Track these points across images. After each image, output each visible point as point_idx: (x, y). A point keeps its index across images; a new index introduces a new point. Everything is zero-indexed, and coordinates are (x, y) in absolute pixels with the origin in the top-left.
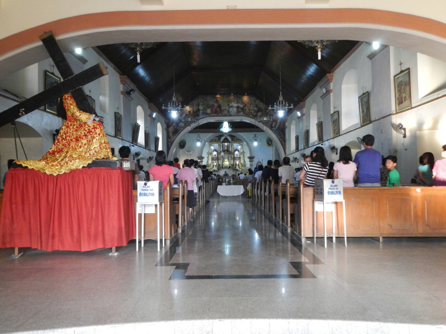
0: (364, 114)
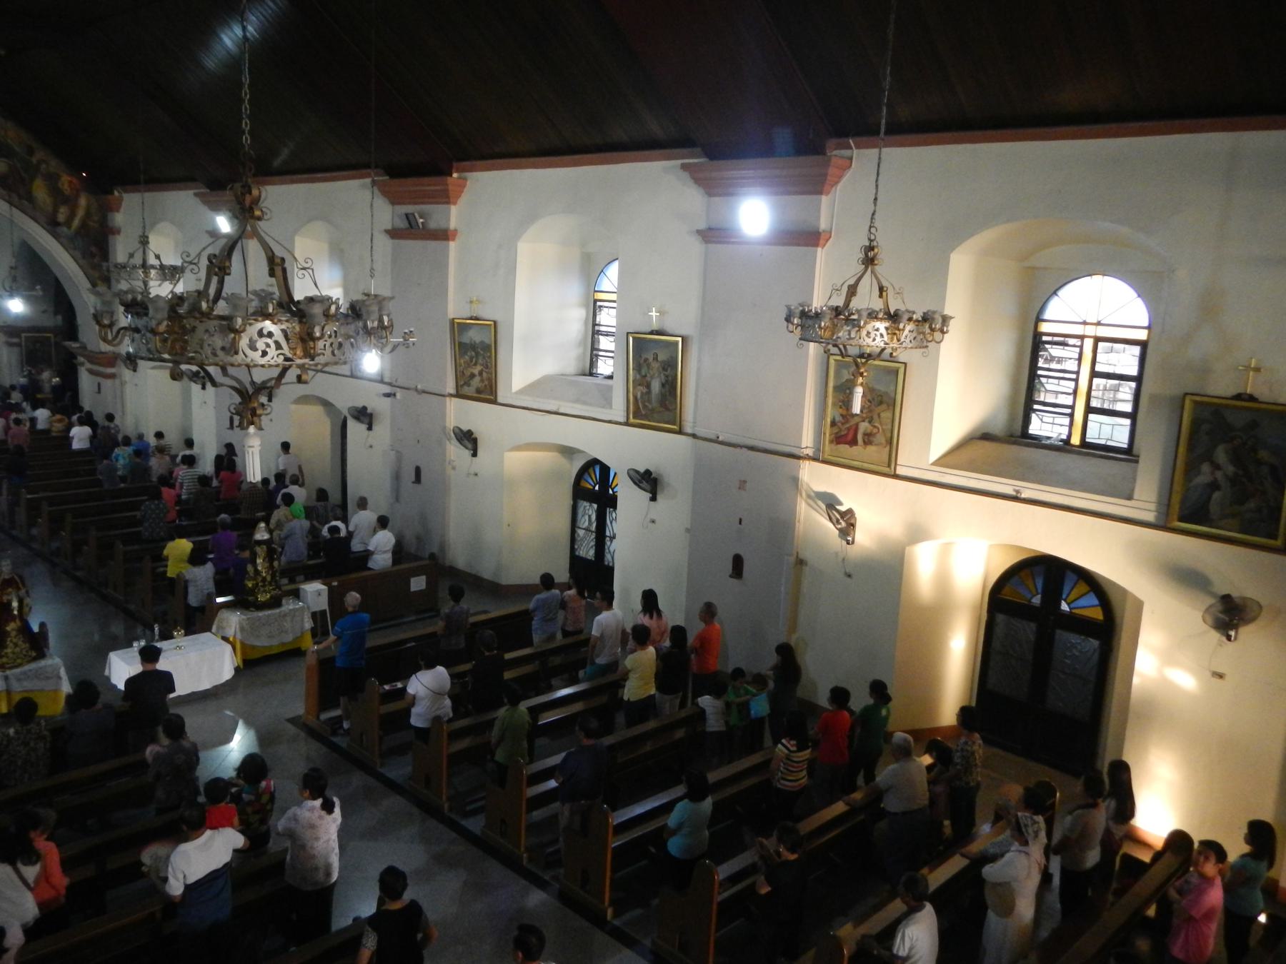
0: (649, 392)
